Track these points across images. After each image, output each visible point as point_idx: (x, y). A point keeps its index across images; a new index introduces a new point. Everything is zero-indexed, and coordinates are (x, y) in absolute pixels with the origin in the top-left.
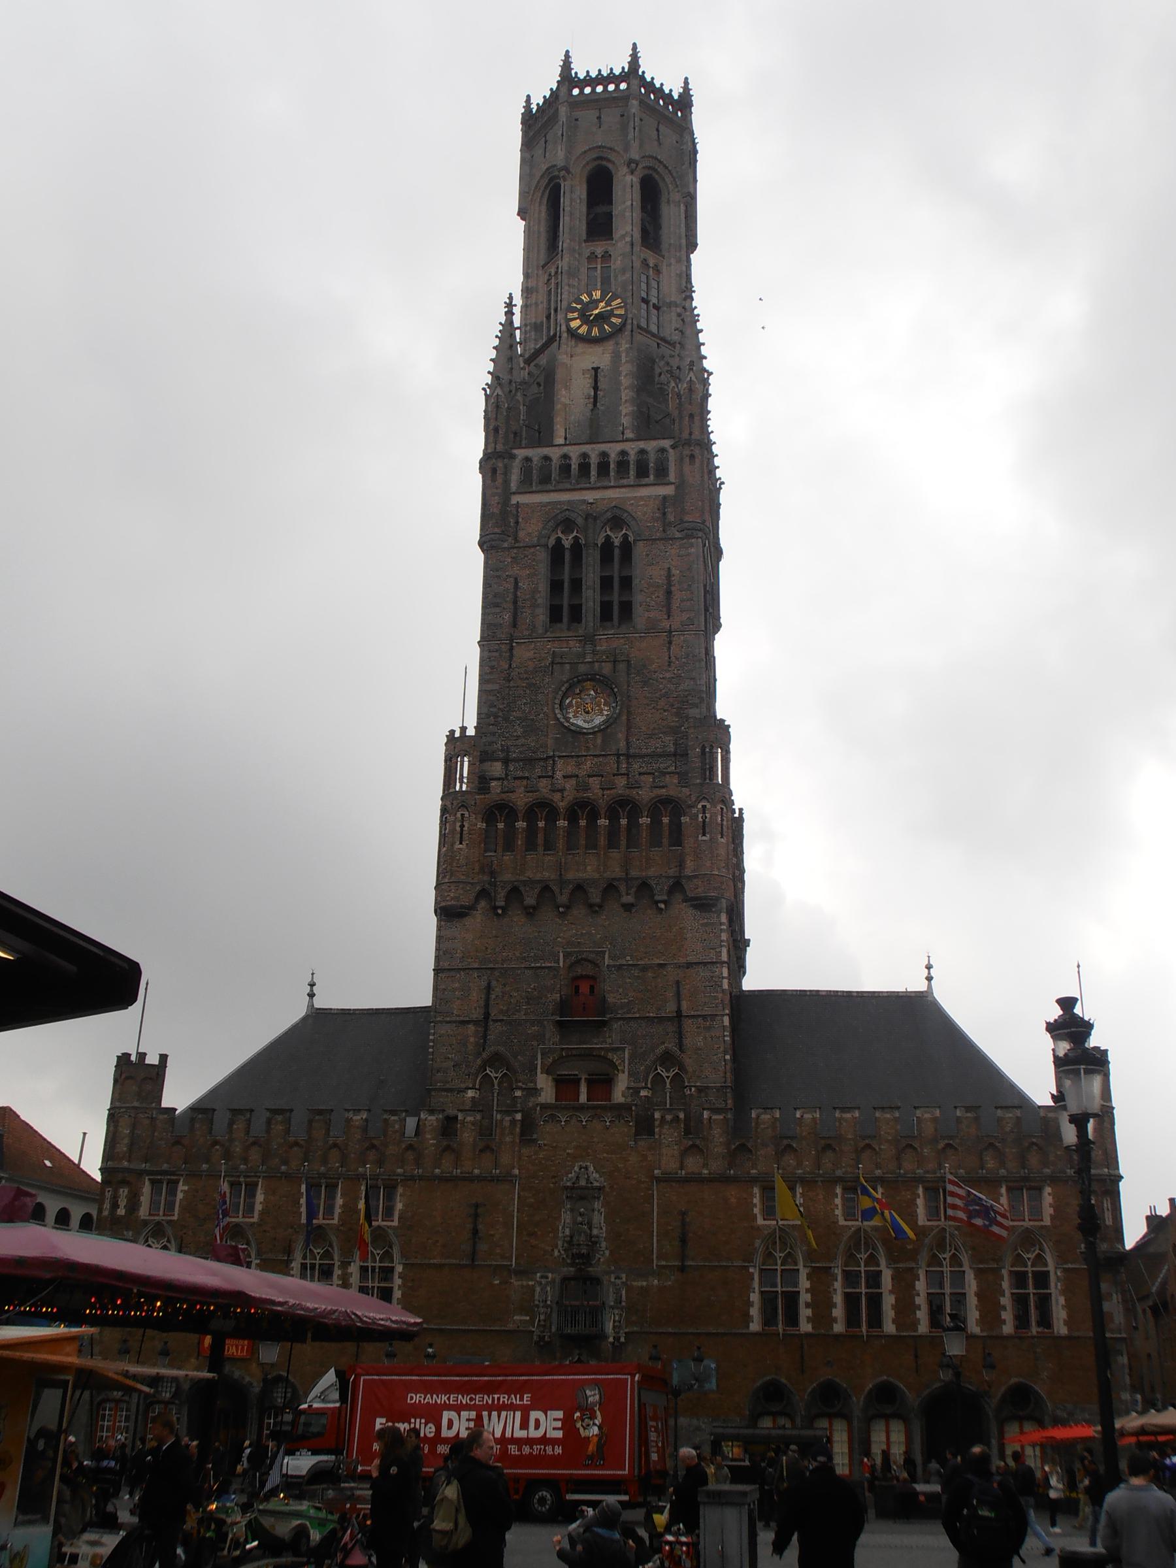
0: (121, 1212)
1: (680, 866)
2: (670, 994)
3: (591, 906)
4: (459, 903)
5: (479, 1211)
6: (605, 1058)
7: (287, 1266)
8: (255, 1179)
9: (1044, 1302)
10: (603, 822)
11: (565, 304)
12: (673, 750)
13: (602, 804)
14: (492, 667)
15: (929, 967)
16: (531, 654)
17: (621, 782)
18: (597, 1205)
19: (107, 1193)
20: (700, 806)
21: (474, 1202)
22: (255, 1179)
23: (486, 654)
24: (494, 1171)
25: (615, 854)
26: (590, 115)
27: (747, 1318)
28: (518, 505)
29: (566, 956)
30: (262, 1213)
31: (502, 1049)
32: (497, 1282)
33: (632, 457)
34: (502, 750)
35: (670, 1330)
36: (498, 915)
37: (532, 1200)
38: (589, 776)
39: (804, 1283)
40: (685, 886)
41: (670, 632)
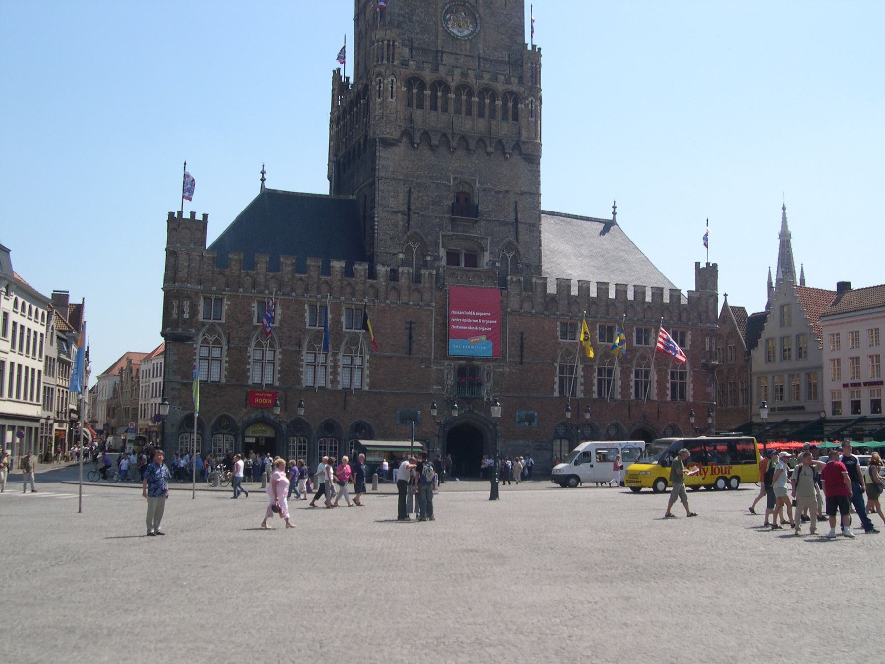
0: (186, 316)
1: (519, 133)
2: (512, 209)
4: (392, 137)
5: (413, 325)
7: (299, 354)
9: (683, 386)
10: (475, 99)
12: (508, 60)
15: (614, 207)
19: (174, 304)
20: (530, 99)
21: (409, 320)
24: (421, 304)
25: (482, 120)
27: (553, 390)
29: (455, 179)
30: (281, 321)
31: (419, 231)
32: (424, 367)
34: (408, 40)
35: (515, 395)
36: (414, 148)
38: (468, 69)
40: (522, 147)
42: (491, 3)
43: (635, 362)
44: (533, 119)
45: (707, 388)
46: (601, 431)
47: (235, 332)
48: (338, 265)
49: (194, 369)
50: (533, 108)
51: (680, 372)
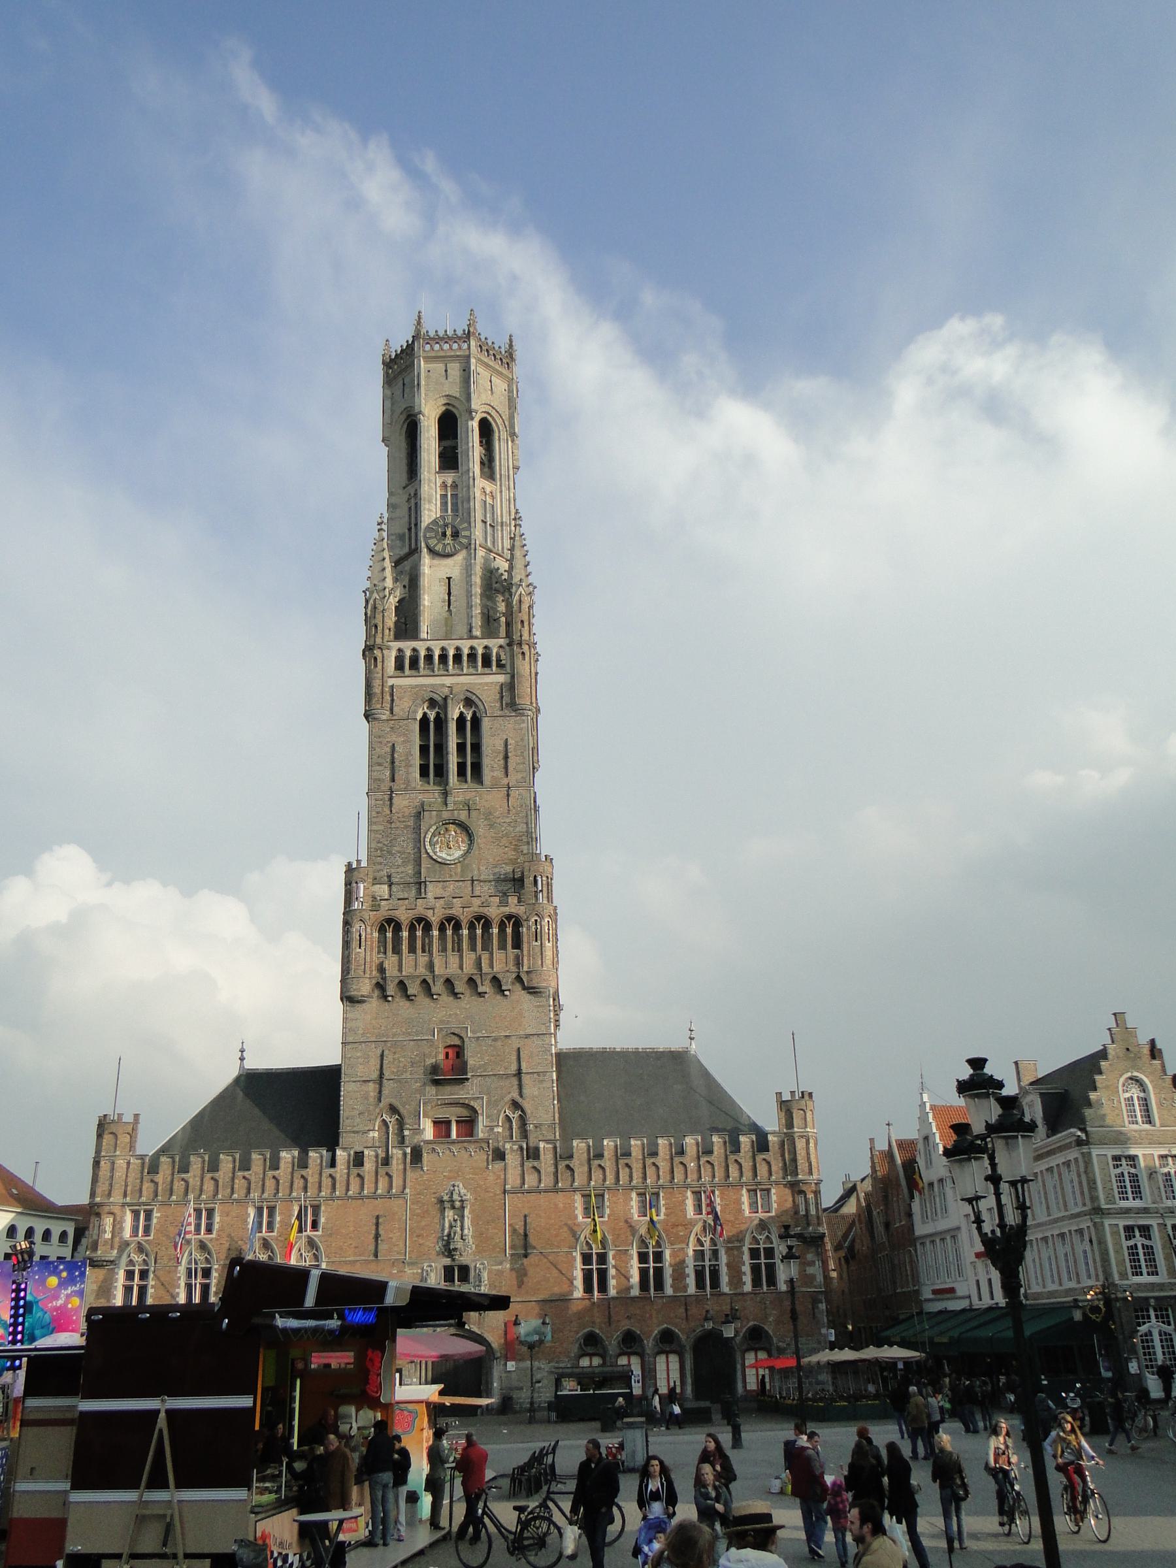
0: (108, 1236)
2: (514, 1058)
3: (457, 994)
5: (380, 1220)
6: (468, 1105)
8: (213, 1205)
11: (424, 525)
13: (465, 918)
14: (378, 813)
16: (406, 803)
17: (476, 902)
18: (466, 1212)
22: (213, 1205)
23: (373, 802)
26: (440, 367)
28: (392, 687)
29: (440, 1030)
33: (480, 651)
36: (389, 1001)
37: (419, 1211)
39: (611, 1261)
41: (509, 788)
42: (490, 813)
43: (692, 1239)
44: (539, 943)
45: (807, 1268)
46: (645, 1341)
47: (164, 1249)
48: (287, 1156)
49: (115, 1299)
50: (538, 930)
51: (764, 1248)
